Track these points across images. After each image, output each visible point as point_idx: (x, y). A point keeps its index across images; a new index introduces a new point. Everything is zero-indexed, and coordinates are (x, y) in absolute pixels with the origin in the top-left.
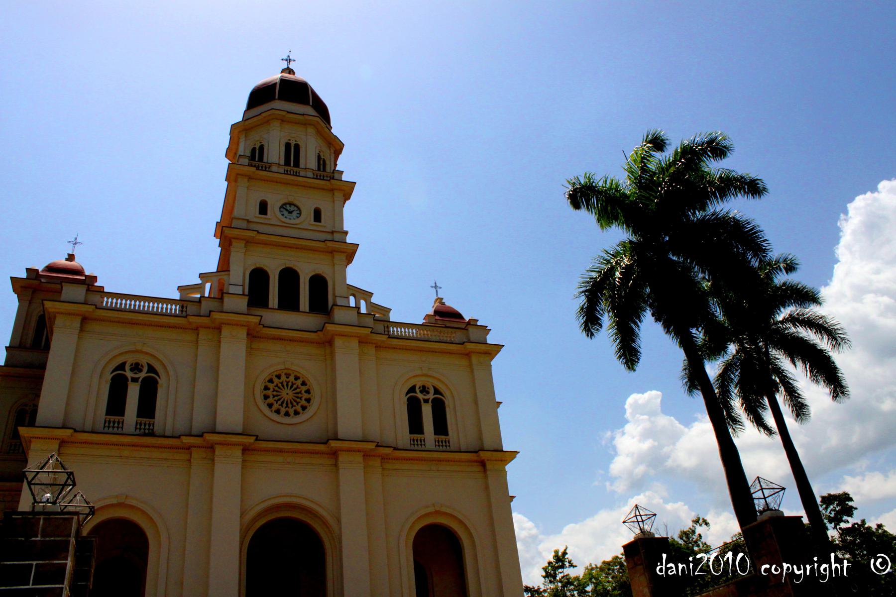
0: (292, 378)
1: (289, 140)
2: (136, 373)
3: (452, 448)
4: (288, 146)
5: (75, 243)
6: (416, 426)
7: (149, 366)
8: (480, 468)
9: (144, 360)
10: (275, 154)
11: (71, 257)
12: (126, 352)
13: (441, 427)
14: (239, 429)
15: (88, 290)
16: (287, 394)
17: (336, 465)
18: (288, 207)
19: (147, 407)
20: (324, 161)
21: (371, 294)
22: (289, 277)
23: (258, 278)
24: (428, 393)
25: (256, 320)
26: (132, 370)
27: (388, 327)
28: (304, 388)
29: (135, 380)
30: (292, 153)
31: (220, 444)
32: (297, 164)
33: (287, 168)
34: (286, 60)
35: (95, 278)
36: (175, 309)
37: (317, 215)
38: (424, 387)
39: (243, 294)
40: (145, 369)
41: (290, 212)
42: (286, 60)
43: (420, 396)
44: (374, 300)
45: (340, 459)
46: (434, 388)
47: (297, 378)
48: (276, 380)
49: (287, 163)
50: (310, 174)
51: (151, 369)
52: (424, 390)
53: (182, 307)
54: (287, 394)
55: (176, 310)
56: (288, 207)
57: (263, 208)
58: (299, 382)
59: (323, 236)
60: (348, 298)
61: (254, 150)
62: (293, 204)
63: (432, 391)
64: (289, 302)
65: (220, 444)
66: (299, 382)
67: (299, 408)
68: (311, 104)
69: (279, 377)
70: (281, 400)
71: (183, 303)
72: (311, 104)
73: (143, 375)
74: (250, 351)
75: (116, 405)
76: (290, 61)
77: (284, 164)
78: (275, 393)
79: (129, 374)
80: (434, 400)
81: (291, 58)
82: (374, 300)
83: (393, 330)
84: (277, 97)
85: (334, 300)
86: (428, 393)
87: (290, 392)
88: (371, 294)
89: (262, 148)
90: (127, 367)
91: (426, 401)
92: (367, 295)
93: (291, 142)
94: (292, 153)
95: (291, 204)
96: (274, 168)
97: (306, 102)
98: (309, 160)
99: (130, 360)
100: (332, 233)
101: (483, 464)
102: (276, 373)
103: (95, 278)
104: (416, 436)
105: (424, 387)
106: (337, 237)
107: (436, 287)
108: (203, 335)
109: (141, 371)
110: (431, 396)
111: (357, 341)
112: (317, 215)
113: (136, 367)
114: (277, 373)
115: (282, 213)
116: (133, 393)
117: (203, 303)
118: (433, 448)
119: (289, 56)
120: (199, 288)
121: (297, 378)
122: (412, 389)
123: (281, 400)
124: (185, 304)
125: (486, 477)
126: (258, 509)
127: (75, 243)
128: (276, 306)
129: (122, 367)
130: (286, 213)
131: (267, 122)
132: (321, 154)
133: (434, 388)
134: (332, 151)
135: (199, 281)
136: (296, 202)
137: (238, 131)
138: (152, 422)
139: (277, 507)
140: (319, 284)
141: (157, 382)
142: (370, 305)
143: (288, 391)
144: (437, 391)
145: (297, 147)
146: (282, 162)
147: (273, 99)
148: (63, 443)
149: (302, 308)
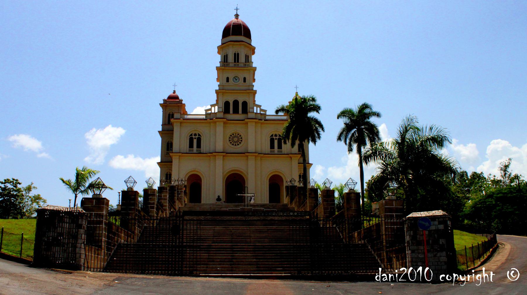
0: (237, 135)
3: (283, 153)
4: (235, 54)
5: (175, 86)
6: (272, 147)
7: (199, 134)
8: (290, 159)
9: (197, 133)
10: (231, 59)
11: (174, 92)
12: (192, 131)
14: (222, 151)
15: (181, 114)
16: (236, 139)
17: (247, 159)
18: (236, 78)
19: (199, 146)
20: (248, 56)
22: (236, 103)
23: (227, 104)
24: (277, 136)
26: (194, 135)
27: (266, 117)
28: (240, 137)
30: (237, 57)
31: (218, 155)
32: (238, 62)
35: (182, 100)
36: (204, 117)
37: (245, 79)
38: (276, 134)
39: (222, 112)
40: (198, 135)
41: (236, 80)
44: (262, 108)
45: (249, 158)
46: (279, 134)
47: (238, 134)
48: (232, 135)
49: (235, 62)
50: (242, 65)
51: (199, 135)
53: (206, 116)
56: (236, 78)
60: (253, 108)
61: (225, 55)
62: (237, 77)
63: (278, 136)
64: (236, 111)
65: (218, 155)
66: (239, 136)
69: (233, 134)
71: (206, 114)
73: (197, 137)
74: (224, 127)
75: (191, 145)
80: (279, 139)
81: (238, 8)
82: (262, 108)
83: (267, 118)
85: (249, 111)
86: (277, 136)
89: (227, 55)
90: (193, 135)
92: (260, 106)
93: (236, 53)
94: (237, 57)
95: (236, 77)
98: (242, 59)
99: (194, 133)
100: (249, 86)
101: (291, 157)
103: (182, 100)
104: (272, 150)
105: (276, 134)
106: (250, 88)
107: (296, 87)
108: (212, 124)
109: (196, 135)
112: (245, 79)
113: (195, 135)
116: (195, 141)
117: (211, 115)
119: (237, 7)
120: (210, 109)
121: (238, 134)
125: (291, 162)
126: (228, 171)
129: (191, 135)
130: (235, 80)
131: (228, 46)
132: (247, 55)
133: (279, 134)
134: (251, 50)
135: (209, 107)
136: (238, 76)
137: (220, 49)
139: (232, 171)
140: (245, 104)
141: (201, 138)
143: (235, 138)
145: (238, 54)
146: (233, 61)
147: (230, 35)
148: (180, 156)
149: (240, 113)
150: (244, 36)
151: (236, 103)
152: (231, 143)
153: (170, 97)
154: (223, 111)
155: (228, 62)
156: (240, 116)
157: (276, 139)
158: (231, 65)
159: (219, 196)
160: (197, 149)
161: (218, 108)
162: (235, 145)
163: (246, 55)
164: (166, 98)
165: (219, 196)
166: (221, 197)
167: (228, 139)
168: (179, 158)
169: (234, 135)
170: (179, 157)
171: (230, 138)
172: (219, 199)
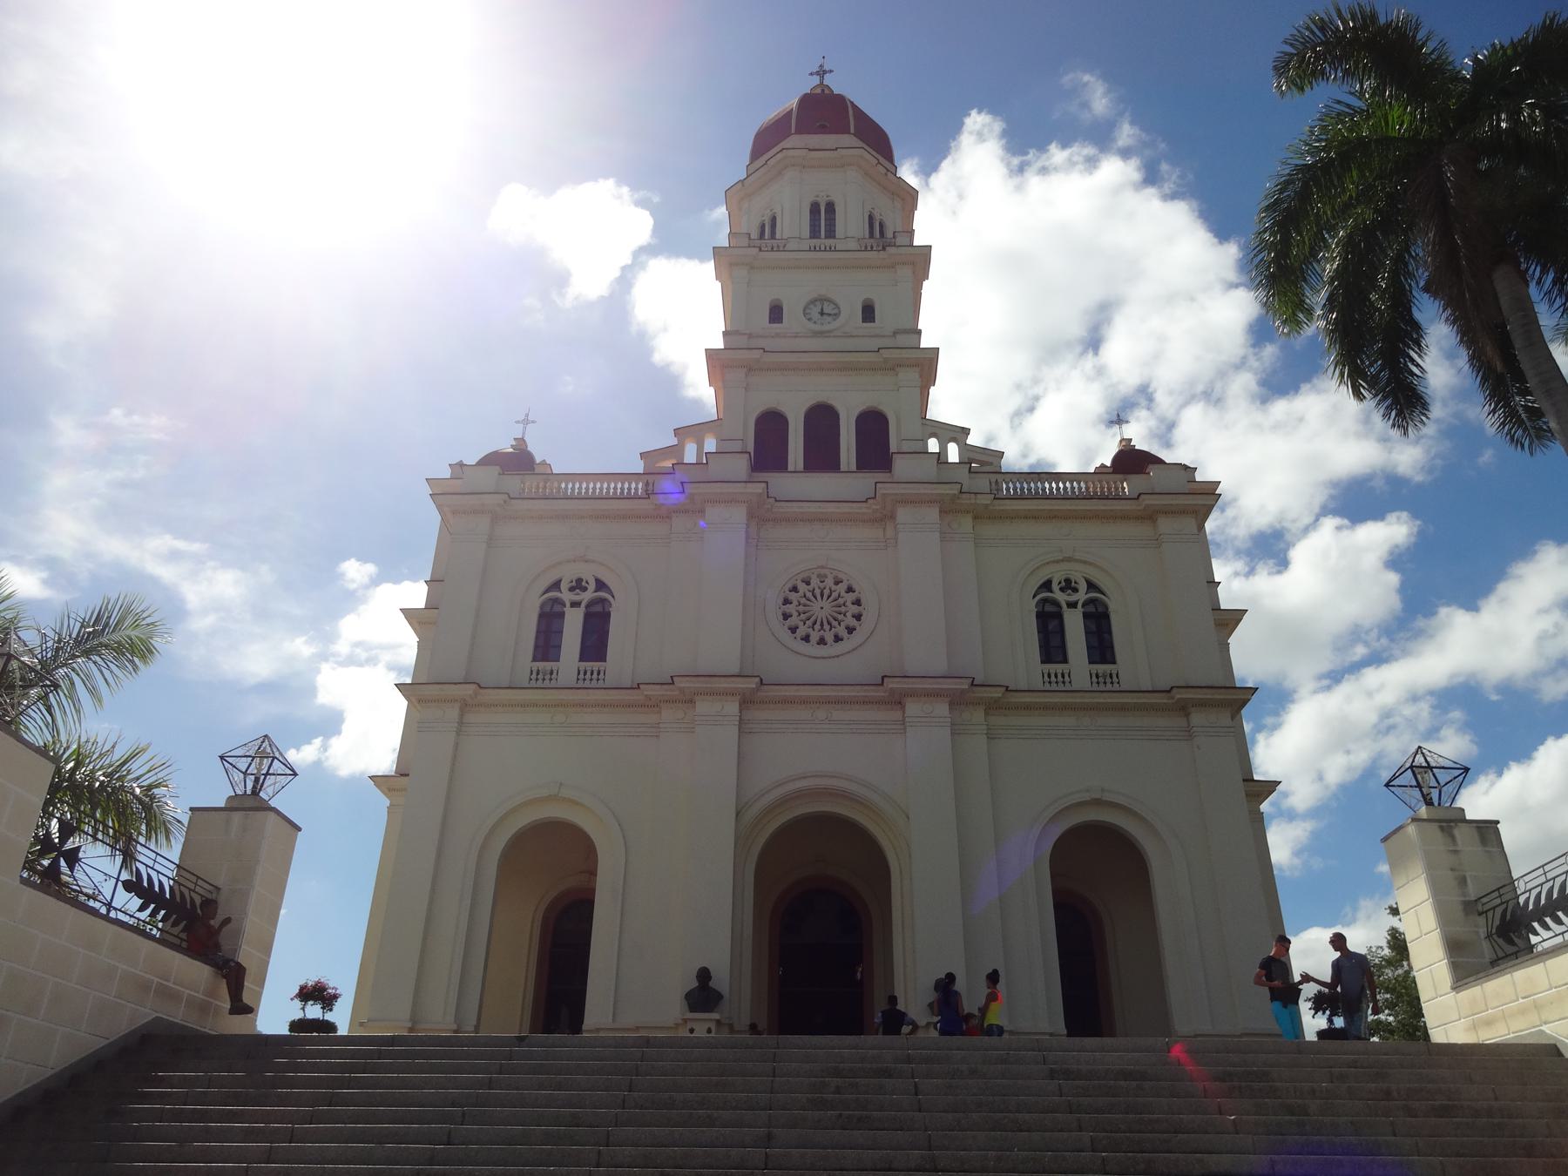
0: (829, 582)
1: (817, 196)
2: (578, 594)
4: (815, 209)
10: (793, 224)
13: (1101, 648)
14: (735, 670)
16: (821, 609)
18: (823, 307)
20: (881, 225)
21: (965, 431)
22: (822, 419)
23: (770, 427)
24: (1075, 590)
25: (758, 488)
29: (575, 604)
30: (822, 217)
32: (831, 233)
33: (814, 242)
34: (817, 73)
37: (868, 312)
38: (1068, 581)
40: (592, 586)
42: (817, 73)
43: (1061, 597)
48: (802, 587)
49: (814, 233)
50: (853, 245)
51: (601, 586)
52: (1068, 586)
53: (647, 484)
54: (822, 608)
55: (636, 489)
56: (823, 307)
57: (776, 313)
58: (842, 588)
59: (874, 344)
61: (763, 227)
63: (1083, 586)
64: (822, 456)
66: (842, 588)
67: (842, 631)
68: (852, 131)
70: (818, 623)
72: (852, 131)
75: (547, 646)
76: (825, 72)
77: (808, 236)
78: (801, 608)
79: (567, 596)
84: (793, 131)
86: (1075, 590)
87: (826, 604)
88: (965, 431)
89: (774, 220)
90: (564, 586)
91: (1072, 605)
92: (960, 434)
96: (790, 246)
97: (843, 129)
98: (850, 224)
99: (568, 574)
102: (801, 576)
105: (1068, 581)
109: (585, 589)
110: (1082, 596)
111: (937, 510)
112: (868, 312)
113: (579, 585)
114: (804, 575)
115: (808, 317)
118: (1087, 686)
119: (821, 66)
122: (1047, 585)
123: (818, 623)
124: (651, 479)
127: (526, 421)
128: (801, 466)
129: (556, 585)
132: (877, 217)
135: (674, 441)
138: (603, 668)
139: (800, 795)
140: (873, 426)
142: (965, 448)
143: (820, 603)
144: (1091, 586)
145: (831, 207)
149: (843, 467)
150: (854, 135)
151: (822, 419)
152: (793, 630)
153: (491, 460)
154: (751, 447)
155: (778, 236)
156: (848, 484)
157: (1072, 605)
158: (792, 245)
159: (704, 975)
160: (584, 664)
161: (720, 440)
162: (822, 641)
163: (871, 218)
164: (471, 460)
165: (704, 975)
166: (721, 980)
167: (774, 609)
168: (461, 723)
169: (815, 582)
170: (462, 715)
171: (787, 602)
172: (703, 995)
